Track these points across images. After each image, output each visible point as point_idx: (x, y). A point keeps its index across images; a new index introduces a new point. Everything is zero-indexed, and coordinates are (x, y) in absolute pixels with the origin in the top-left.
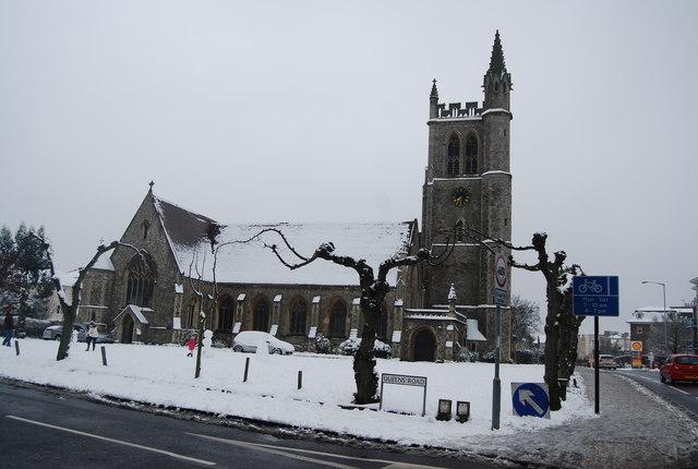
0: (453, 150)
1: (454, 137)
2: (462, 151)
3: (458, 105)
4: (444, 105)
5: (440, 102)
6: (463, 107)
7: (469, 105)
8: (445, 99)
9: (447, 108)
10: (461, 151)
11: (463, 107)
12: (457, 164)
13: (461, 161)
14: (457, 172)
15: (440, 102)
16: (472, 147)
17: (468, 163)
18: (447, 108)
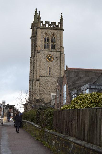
0: (46, 40)
1: (47, 34)
2: (50, 41)
3: (48, 23)
4: (42, 22)
5: (41, 20)
6: (50, 23)
7: (53, 23)
8: (44, 19)
9: (44, 23)
11: (50, 23)
12: (48, 45)
13: (50, 44)
14: (48, 48)
15: (41, 20)
16: (53, 40)
17: (52, 45)
18: (44, 23)
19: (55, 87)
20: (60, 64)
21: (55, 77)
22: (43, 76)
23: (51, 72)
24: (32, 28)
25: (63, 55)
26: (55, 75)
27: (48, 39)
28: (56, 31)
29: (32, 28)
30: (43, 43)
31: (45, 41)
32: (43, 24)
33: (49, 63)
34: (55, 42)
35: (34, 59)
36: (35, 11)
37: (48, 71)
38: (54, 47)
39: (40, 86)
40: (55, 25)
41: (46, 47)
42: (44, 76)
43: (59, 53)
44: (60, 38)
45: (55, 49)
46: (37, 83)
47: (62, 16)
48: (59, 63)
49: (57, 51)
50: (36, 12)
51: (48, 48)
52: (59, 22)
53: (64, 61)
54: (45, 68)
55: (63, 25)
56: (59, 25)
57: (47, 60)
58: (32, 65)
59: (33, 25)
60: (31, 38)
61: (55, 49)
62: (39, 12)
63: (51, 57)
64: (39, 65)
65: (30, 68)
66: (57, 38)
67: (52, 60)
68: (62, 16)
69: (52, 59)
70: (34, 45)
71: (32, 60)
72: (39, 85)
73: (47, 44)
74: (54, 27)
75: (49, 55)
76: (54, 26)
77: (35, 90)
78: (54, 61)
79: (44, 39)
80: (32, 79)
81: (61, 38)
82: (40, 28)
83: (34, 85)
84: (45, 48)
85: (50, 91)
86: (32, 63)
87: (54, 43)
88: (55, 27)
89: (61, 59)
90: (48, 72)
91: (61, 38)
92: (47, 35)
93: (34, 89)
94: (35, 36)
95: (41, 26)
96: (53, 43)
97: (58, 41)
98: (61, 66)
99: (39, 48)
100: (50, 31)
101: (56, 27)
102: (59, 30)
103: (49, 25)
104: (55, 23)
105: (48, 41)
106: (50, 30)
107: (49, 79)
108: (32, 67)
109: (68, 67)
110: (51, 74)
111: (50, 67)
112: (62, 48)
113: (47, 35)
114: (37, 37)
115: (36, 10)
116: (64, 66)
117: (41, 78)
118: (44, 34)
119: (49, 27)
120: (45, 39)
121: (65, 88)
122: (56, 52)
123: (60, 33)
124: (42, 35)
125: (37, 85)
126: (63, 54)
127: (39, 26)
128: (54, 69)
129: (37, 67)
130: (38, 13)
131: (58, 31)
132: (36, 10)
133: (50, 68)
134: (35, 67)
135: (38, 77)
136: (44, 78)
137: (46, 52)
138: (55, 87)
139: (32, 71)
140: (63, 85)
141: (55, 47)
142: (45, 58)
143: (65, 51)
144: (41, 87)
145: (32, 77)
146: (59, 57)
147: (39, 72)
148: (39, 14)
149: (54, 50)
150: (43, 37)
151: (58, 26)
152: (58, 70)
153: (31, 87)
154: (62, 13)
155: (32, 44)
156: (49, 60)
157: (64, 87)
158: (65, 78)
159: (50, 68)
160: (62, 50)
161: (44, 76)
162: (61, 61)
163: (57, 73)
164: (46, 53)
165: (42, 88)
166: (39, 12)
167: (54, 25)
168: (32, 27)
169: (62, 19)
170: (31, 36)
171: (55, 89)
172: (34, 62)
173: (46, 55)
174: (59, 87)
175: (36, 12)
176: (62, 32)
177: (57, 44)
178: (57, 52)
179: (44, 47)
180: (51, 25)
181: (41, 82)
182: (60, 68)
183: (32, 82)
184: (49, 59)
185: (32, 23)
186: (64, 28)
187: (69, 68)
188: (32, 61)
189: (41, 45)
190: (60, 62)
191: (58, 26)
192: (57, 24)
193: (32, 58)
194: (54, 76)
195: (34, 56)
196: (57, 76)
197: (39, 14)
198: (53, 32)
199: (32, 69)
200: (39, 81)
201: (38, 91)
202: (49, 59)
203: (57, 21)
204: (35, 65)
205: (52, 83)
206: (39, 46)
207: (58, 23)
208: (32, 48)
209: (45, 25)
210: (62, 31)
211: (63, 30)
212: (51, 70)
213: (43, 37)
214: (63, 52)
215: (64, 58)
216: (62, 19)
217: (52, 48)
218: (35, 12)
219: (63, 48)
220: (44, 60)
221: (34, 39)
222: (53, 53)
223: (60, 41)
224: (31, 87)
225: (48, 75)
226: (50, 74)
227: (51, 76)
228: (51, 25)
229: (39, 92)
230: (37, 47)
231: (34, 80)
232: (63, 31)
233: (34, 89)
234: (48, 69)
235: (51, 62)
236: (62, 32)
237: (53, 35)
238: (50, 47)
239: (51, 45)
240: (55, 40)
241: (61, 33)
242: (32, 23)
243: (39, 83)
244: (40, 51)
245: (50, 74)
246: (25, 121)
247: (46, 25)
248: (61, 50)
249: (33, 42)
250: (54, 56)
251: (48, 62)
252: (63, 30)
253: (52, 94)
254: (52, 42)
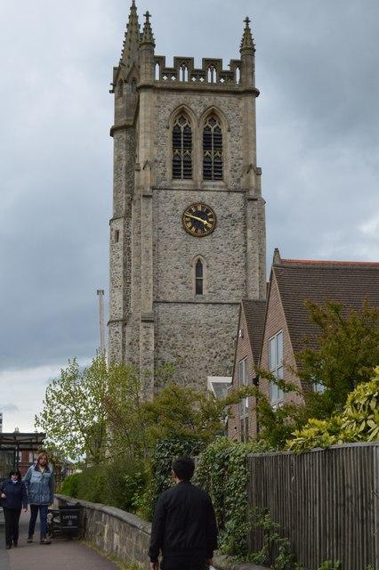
0: (181, 139)
1: (182, 113)
2: (198, 144)
4: (161, 60)
5: (157, 52)
6: (198, 65)
8: (167, 47)
9: (170, 64)
10: (198, 144)
11: (198, 65)
12: (188, 164)
14: (188, 175)
15: (155, 54)
16: (213, 141)
17: (206, 162)
18: (170, 64)
19: (225, 347)
20: (245, 245)
21: (223, 304)
22: (169, 299)
23: (205, 283)
24: (117, 89)
25: (256, 203)
26: (224, 295)
27: (188, 134)
28: (223, 102)
29: (117, 89)
30: (168, 152)
31: (176, 144)
32: (165, 71)
33: (197, 240)
34: (219, 146)
35: (127, 225)
36: (129, 12)
37: (194, 276)
38: (213, 171)
39: (156, 345)
40: (222, 74)
41: (181, 169)
42: (176, 303)
43: (238, 197)
44: (242, 128)
45: (220, 178)
46: (143, 332)
47: (247, 30)
48: (240, 239)
49: (232, 188)
50: (133, 16)
51: (188, 175)
52: (238, 57)
53: (264, 229)
54: (178, 264)
55: (253, 73)
56: (238, 70)
57: (184, 228)
58: (121, 253)
59: (121, 77)
60: (112, 135)
61: (220, 178)
62: (147, 15)
63: (202, 214)
64: (151, 252)
65: (112, 265)
66: (229, 131)
67: (208, 228)
68: (247, 30)
69: (210, 226)
70: (124, 163)
71: (118, 232)
72: (152, 340)
73: (187, 159)
74: (215, 81)
75: (195, 205)
76: (212, 77)
77: (134, 363)
78: (219, 232)
79: (169, 134)
80: (120, 314)
81: (246, 130)
82: (146, 87)
83: (128, 340)
84: (176, 174)
85: (203, 365)
86: (121, 243)
87: (218, 154)
88: (218, 80)
89: (250, 222)
90: (194, 282)
91: (246, 130)
92: (182, 120)
93: (130, 359)
94: (131, 123)
95: (157, 78)
96: (212, 154)
98: (251, 256)
99: (144, 178)
100: (199, 97)
101: (222, 80)
102: (236, 93)
103: (194, 73)
104: (212, 63)
105: (188, 145)
106: (198, 97)
107: (198, 313)
108: (120, 261)
109: (286, 255)
110: (205, 292)
111: (199, 260)
112: (252, 172)
113: (182, 120)
114: (142, 129)
115: (133, 8)
116: (262, 255)
117: (161, 307)
118: (168, 114)
119: (194, 83)
120: (176, 135)
121: (278, 350)
122: (226, 194)
124: (161, 117)
125: (142, 340)
126: (256, 200)
127: (143, 81)
128: (221, 267)
129: (143, 263)
130: (142, 21)
131: (234, 99)
132: (133, 8)
133: (199, 266)
134: (134, 260)
135: (148, 308)
136: (174, 308)
137: (182, 193)
138: (225, 347)
139: (120, 282)
140: (267, 333)
141: (221, 172)
142: (180, 220)
143: (271, 189)
144: (161, 350)
145: (121, 305)
146: (240, 215)
147: (151, 281)
148: (147, 24)
149: (218, 183)
150: (168, 128)
151: (230, 75)
152: (236, 273)
153: (116, 350)
154: (247, 21)
155: (118, 160)
156: (194, 229)
157: (273, 343)
158: (276, 297)
159: (199, 266)
160: (253, 183)
161: (176, 303)
162: (249, 232)
163: (232, 286)
164: (182, 195)
165: (166, 355)
166: (147, 15)
167: (215, 73)
168: (114, 85)
169: (248, 48)
170: (111, 123)
171: (225, 358)
172: (127, 240)
173: (181, 208)
174: (246, 348)
175: (133, 16)
176: (249, 103)
177: (229, 155)
178: (229, 191)
179: (169, 170)
180: (202, 73)
181: (162, 329)
182: (246, 267)
183: (119, 328)
184: (199, 221)
185: (115, 69)
186: (258, 86)
187: (282, 261)
188: (121, 236)
189: (156, 161)
190: (246, 237)
191: (230, 75)
192: (226, 67)
193: (119, 225)
194: (223, 301)
195: (128, 215)
196: (234, 300)
197: (147, 24)
198: (210, 103)
199: (121, 269)
200: (152, 325)
201: (151, 368)
202: (199, 221)
203: (229, 53)
204: (132, 246)
205: (213, 330)
206: (148, 168)
207: (234, 63)
208: (115, 180)
209: (173, 72)
210: (249, 99)
211: (256, 93)
212: (205, 271)
213: (168, 128)
214: (258, 190)
215: (261, 217)
216: (248, 48)
217: (207, 176)
218: (127, 21)
219: (258, 172)
220: (174, 229)
221: (124, 135)
222: (211, 195)
223: (241, 141)
224: (116, 350)
225: (191, 294)
226: (199, 290)
227: (207, 300)
228: (202, 73)
229: (152, 371)
230: (139, 170)
231: (132, 320)
232: (257, 99)
233: (130, 359)
234: (193, 270)
235: (207, 239)
236: (253, 103)
237: (213, 115)
238: (200, 172)
239: (204, 162)
240: (219, 138)
241: (246, 104)
242: (115, 69)
243: (152, 331)
244: (153, 188)
245: (199, 290)
246: (98, 506)
247: (176, 75)
248: (249, 180)
249: (124, 153)
250: (218, 212)
251: (192, 239)
252: (256, 93)
253: (212, 379)
254: (207, 146)
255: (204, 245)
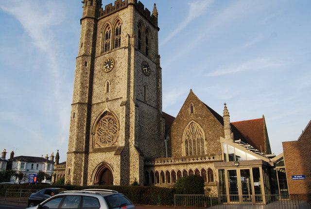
28: (151, 28)
33: (145, 77)
70: (92, 33)
78: (150, 76)
97: (153, 45)
104: (148, 12)
108: (88, 76)
123: (155, 32)
152: (154, 95)
154: (155, 4)
155: (89, 30)
173: (142, 60)
205: (149, 117)
211: (158, 29)
232: (159, 32)
237: (147, 30)
255: (146, 80)
